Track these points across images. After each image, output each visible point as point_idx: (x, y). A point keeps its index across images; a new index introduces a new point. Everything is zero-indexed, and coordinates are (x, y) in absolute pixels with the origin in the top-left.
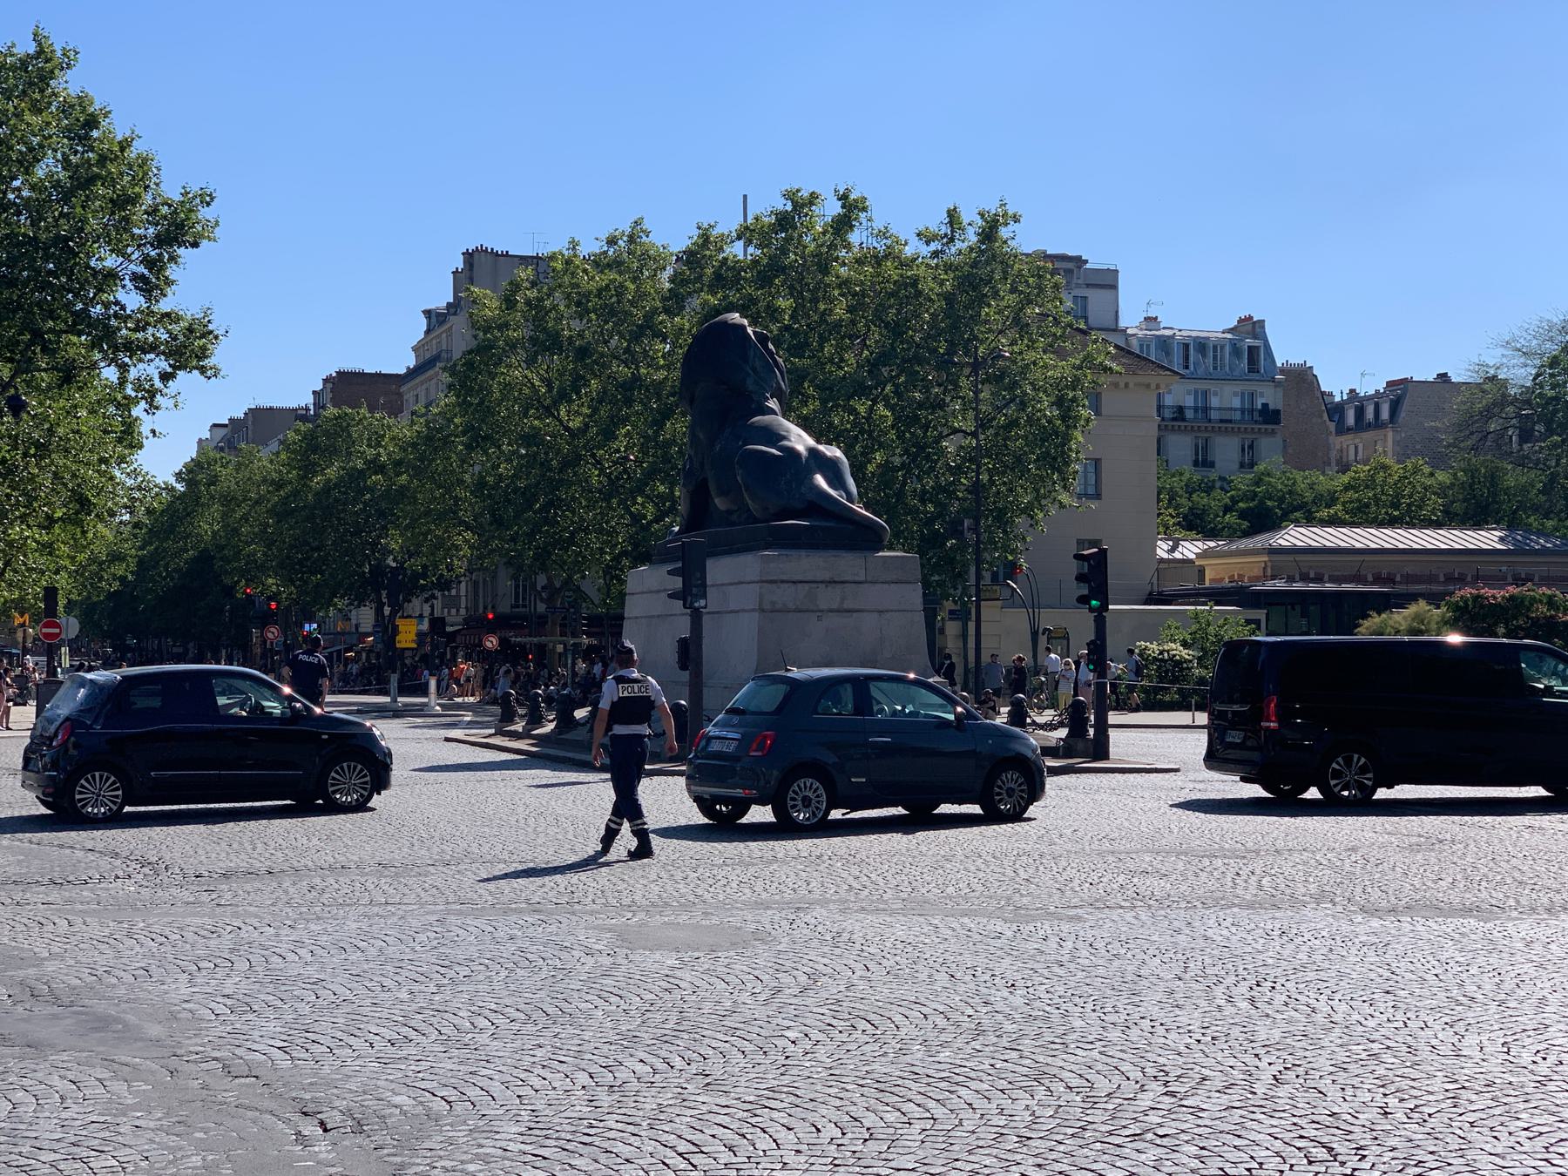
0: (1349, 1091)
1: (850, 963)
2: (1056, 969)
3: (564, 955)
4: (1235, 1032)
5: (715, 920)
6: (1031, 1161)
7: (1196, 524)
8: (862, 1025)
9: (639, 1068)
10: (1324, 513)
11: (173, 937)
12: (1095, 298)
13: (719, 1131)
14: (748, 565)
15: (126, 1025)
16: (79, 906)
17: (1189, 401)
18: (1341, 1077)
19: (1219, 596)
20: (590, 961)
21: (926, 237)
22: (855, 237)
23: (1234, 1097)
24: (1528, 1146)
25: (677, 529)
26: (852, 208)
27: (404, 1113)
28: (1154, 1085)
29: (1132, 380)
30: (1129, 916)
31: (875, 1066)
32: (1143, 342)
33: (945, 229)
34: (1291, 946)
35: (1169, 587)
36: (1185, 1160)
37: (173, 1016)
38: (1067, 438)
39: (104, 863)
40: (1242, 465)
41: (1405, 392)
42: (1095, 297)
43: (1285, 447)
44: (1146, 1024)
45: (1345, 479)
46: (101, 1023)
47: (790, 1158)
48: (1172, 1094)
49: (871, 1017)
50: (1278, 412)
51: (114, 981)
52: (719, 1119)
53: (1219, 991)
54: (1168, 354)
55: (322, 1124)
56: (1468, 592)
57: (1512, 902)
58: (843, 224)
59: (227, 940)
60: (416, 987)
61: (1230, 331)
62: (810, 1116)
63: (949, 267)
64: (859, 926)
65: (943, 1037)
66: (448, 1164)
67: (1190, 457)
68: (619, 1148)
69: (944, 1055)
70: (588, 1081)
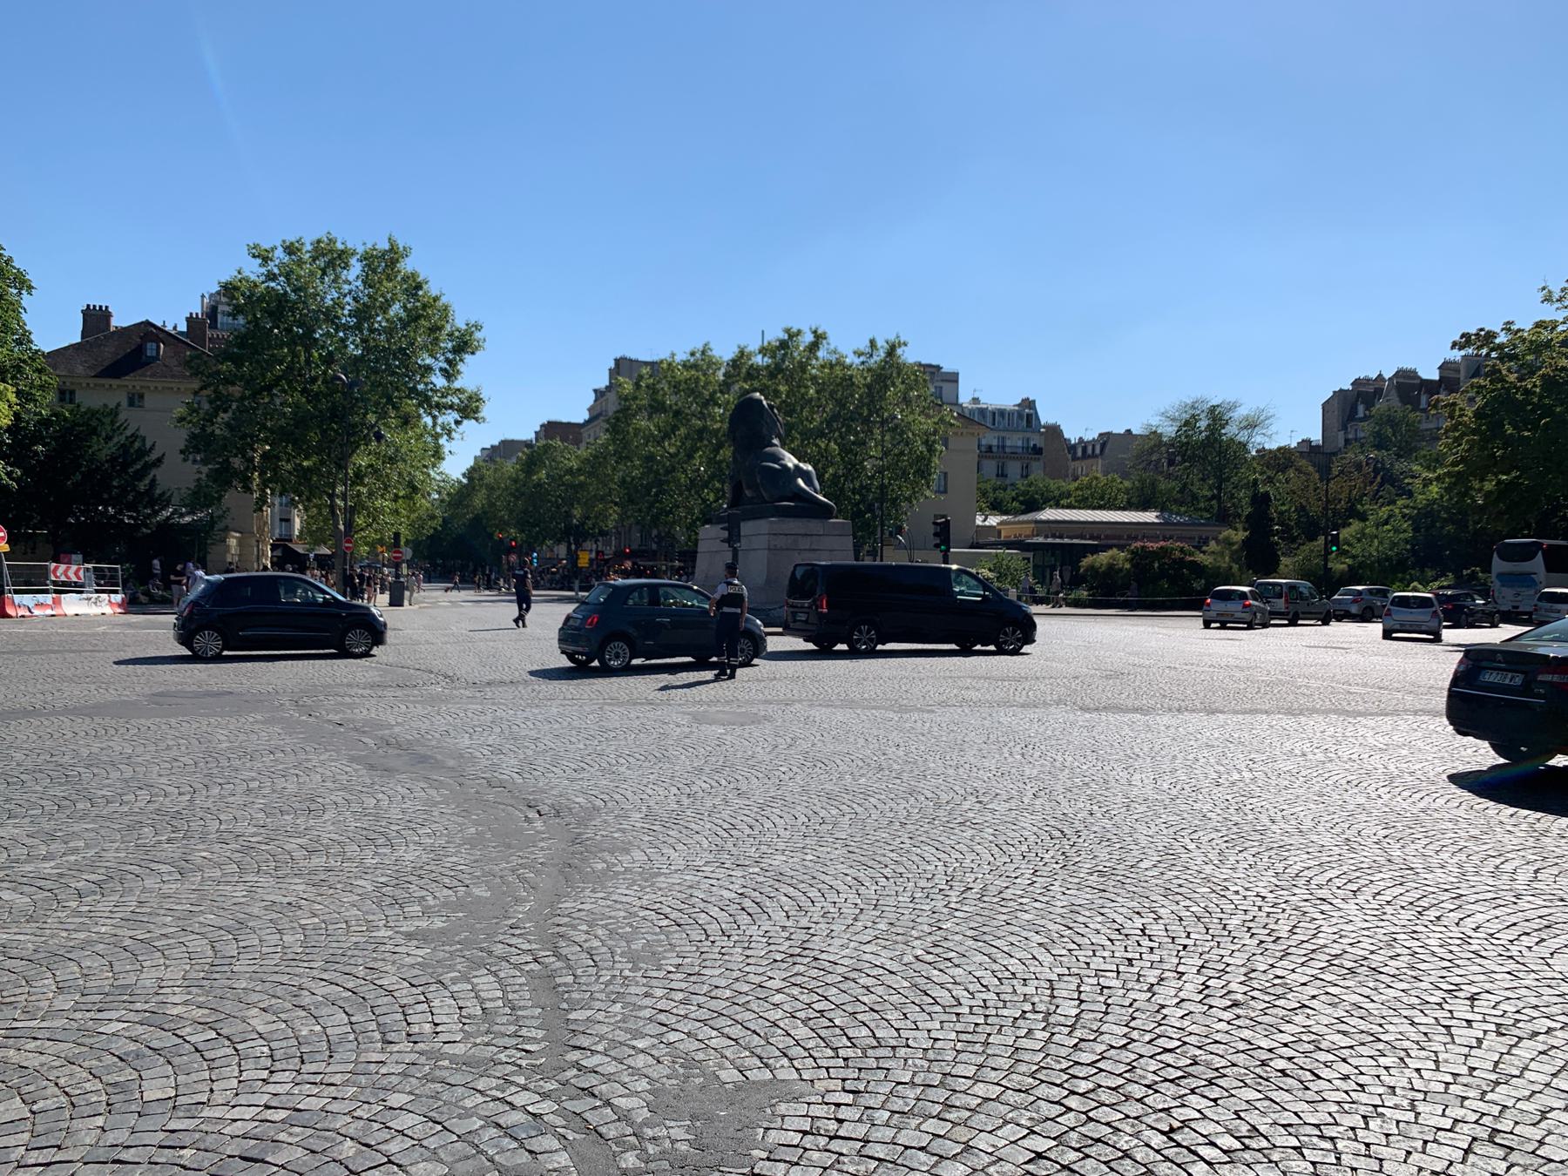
0: (1073, 802)
1: (814, 732)
2: (920, 737)
3: (664, 727)
4: (1013, 770)
5: (744, 710)
6: (906, 835)
7: (997, 507)
8: (819, 765)
9: (704, 785)
11: (461, 715)
13: (745, 818)
14: (763, 525)
15: (436, 760)
16: (411, 698)
17: (995, 443)
18: (1069, 795)
19: (1008, 545)
20: (679, 730)
21: (859, 354)
22: (820, 354)
23: (1013, 804)
24: (1165, 831)
25: (725, 506)
26: (819, 337)
27: (581, 807)
28: (971, 798)
29: (965, 431)
30: (959, 710)
31: (826, 786)
32: (971, 411)
33: (868, 350)
34: (1043, 727)
36: (987, 836)
37: (461, 756)
38: (930, 461)
39: (425, 676)
42: (946, 386)
43: (1045, 467)
44: (967, 766)
46: (423, 759)
47: (782, 832)
48: (980, 802)
49: (827, 762)
50: (1041, 449)
51: (430, 737)
52: (745, 812)
53: (1005, 750)
54: (984, 417)
55: (539, 812)
56: (1139, 544)
57: (1159, 706)
58: (814, 347)
59: (489, 717)
60: (588, 742)
61: (1019, 405)
62: (792, 811)
63: (869, 370)
64: (818, 713)
65: (861, 771)
66: (604, 833)
68: (693, 826)
69: (863, 780)
70: (676, 792)
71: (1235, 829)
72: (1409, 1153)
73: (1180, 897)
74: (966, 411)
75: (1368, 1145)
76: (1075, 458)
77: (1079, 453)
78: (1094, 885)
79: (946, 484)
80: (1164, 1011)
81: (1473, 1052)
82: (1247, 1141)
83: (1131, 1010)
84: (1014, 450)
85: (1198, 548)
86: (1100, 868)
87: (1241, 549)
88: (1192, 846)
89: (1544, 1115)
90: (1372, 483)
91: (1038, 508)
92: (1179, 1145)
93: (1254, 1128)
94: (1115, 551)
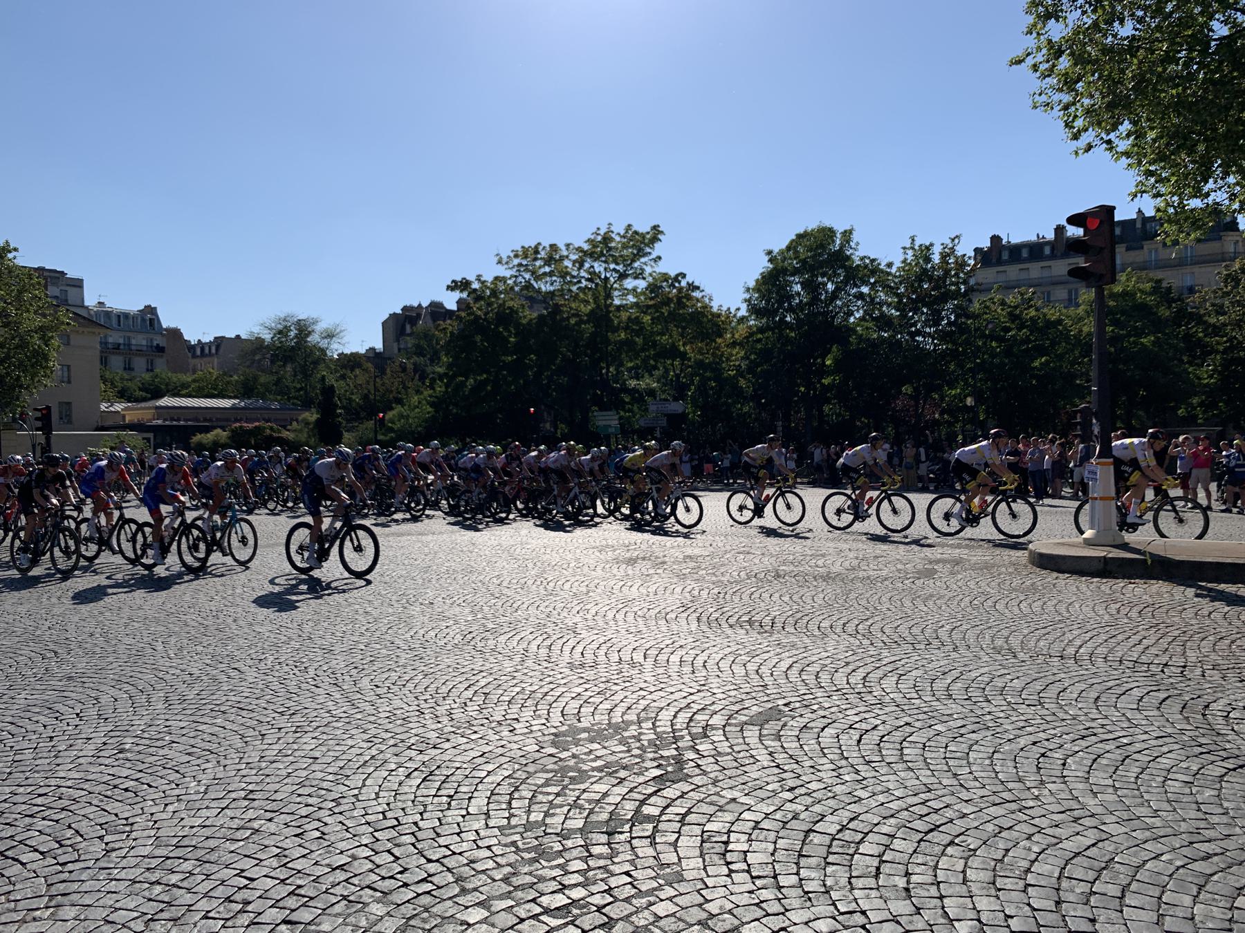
4: (43, 611)
7: (123, 395)
10: (183, 392)
12: (72, 292)
17: (121, 341)
29: (86, 330)
35: (107, 424)
40: (148, 370)
45: (194, 377)
56: (238, 425)
67: (123, 366)
71: (203, 630)
72: (182, 819)
73: (126, 685)
74: (92, 312)
75: (156, 822)
76: (194, 356)
77: (198, 352)
78: (58, 688)
79: (69, 377)
80: (58, 768)
82: (63, 842)
83: (28, 774)
84: (139, 348)
85: (284, 427)
86: (73, 675)
88: (160, 647)
89: (289, 775)
90: (413, 379)
91: (159, 395)
92: (7, 858)
93: (77, 832)
94: (219, 431)
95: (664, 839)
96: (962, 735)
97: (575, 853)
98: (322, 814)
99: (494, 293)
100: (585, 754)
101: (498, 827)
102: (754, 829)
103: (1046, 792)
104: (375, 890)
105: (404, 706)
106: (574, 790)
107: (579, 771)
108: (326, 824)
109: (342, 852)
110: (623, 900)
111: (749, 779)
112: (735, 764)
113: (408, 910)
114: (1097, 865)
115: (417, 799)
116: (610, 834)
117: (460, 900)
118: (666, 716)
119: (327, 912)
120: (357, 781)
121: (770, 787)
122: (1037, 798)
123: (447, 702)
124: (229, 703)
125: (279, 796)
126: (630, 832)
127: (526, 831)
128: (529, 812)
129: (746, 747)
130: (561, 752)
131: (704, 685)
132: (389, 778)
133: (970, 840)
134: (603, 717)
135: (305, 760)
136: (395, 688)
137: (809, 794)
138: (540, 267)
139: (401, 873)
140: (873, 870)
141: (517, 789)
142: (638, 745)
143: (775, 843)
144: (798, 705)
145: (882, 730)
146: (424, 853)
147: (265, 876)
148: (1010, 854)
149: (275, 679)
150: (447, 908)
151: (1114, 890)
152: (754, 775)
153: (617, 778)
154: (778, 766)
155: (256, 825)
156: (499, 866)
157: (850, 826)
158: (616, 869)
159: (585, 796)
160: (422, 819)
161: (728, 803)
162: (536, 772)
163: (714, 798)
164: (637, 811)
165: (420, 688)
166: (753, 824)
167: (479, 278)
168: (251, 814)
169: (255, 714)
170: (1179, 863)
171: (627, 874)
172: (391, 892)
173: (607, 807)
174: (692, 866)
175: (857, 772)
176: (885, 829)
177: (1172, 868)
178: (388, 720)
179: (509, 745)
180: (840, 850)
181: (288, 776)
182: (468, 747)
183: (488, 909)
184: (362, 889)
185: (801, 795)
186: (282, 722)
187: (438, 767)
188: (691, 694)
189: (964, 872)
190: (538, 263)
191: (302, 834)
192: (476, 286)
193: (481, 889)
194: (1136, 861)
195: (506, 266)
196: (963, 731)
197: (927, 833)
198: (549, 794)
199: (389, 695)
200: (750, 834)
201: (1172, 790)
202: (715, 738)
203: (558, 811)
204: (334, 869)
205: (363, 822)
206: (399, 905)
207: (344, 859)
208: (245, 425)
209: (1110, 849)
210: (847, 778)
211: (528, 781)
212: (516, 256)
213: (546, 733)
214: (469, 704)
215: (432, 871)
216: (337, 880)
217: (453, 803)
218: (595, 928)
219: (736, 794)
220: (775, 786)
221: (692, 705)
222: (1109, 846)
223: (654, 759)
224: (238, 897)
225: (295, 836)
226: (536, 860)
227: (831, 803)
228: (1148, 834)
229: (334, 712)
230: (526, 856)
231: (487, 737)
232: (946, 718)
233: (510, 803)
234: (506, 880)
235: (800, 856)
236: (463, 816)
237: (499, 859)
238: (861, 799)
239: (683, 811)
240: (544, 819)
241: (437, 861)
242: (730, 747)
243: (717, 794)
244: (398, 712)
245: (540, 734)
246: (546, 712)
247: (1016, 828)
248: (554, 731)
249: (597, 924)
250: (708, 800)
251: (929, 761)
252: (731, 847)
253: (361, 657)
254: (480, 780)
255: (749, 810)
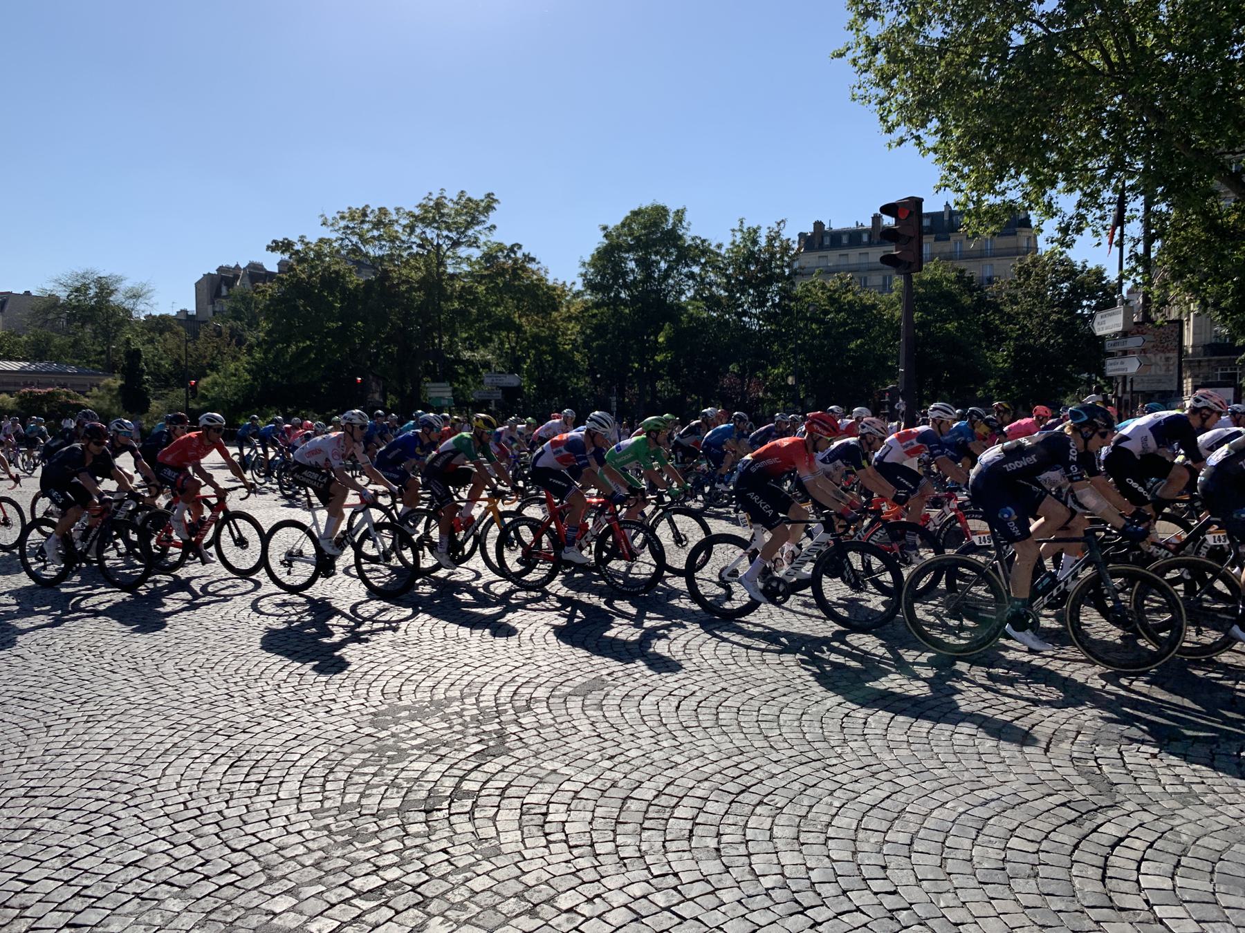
41: (8, 298)
56: (27, 390)
81: (58, 739)
85: (83, 393)
87: (117, 395)
90: (229, 345)
95: (483, 814)
96: (774, 699)
97: (391, 833)
98: (114, 808)
99: (319, 255)
100: (405, 732)
101: (310, 811)
102: (573, 799)
103: (848, 750)
104: (172, 885)
105: (212, 689)
106: (392, 769)
107: (399, 750)
108: (119, 819)
109: (136, 848)
110: (439, 878)
111: (570, 750)
112: (557, 735)
113: (209, 904)
114: (890, 816)
115: (223, 786)
116: (427, 812)
117: (266, 889)
118: (489, 691)
119: (117, 911)
120: (156, 770)
121: (590, 757)
122: (840, 756)
123: (260, 684)
124: (10, 694)
125: (64, 792)
126: (449, 808)
127: (340, 814)
128: (344, 794)
129: (569, 718)
130: (380, 731)
131: (529, 658)
132: (192, 766)
133: (777, 799)
134: (425, 695)
135: (97, 751)
136: (202, 672)
137: (627, 762)
138: (368, 231)
139: (202, 865)
140: (687, 833)
141: (331, 771)
142: (460, 721)
143: (593, 811)
144: (620, 674)
145: (700, 696)
146: (229, 843)
147: (46, 878)
148: (814, 810)
149: (65, 666)
150: (253, 899)
151: (904, 838)
152: (575, 746)
153: (437, 755)
154: (599, 736)
155: (37, 824)
156: (310, 851)
157: (666, 791)
158: (433, 847)
159: (403, 775)
160: (228, 808)
161: (548, 774)
162: (352, 753)
163: (535, 770)
164: (457, 787)
165: (230, 671)
166: (573, 794)
167: (302, 239)
168: (32, 812)
169: (40, 704)
170: (961, 810)
171: (445, 851)
172: (190, 886)
173: (426, 784)
174: (510, 839)
175: (675, 738)
176: (699, 793)
177: (955, 815)
178: (193, 705)
179: (324, 727)
180: (656, 816)
181: (76, 770)
182: (281, 729)
183: (296, 897)
184: (158, 885)
185: (620, 763)
186: (70, 711)
187: (248, 752)
188: (516, 668)
189: (771, 829)
190: (366, 226)
191: (90, 830)
192: (298, 247)
193: (289, 876)
194: (924, 810)
195: (331, 228)
196: (775, 694)
197: (738, 794)
198: (365, 774)
199: (196, 679)
200: (569, 805)
201: (958, 742)
202: (539, 711)
203: (374, 791)
204: (126, 866)
205: (162, 813)
206: (198, 899)
207: (138, 855)
208: (37, 390)
209: (903, 800)
210: (665, 744)
211: (344, 762)
212: (343, 218)
213: (365, 712)
214: (282, 685)
215: (236, 861)
216: (129, 878)
217: (262, 789)
218: (409, 908)
219: (556, 765)
220: (595, 755)
221: (517, 679)
222: (901, 798)
223: (476, 735)
224: (15, 902)
225: (82, 833)
226: (350, 843)
227: (650, 769)
228: (935, 785)
229: (132, 699)
230: (340, 839)
231: (301, 719)
232: (759, 683)
233: (324, 786)
234: (316, 865)
235: (617, 823)
236: (273, 802)
237: (310, 844)
238: (677, 764)
239: (503, 785)
240: (359, 801)
241: (243, 850)
242: (553, 719)
243: (538, 766)
244: (205, 696)
245: (358, 714)
246: (365, 691)
247: (820, 785)
248: (373, 710)
249: (411, 903)
250: (529, 772)
251: (742, 724)
252: (549, 818)
253: (165, 639)
254: (292, 763)
255: (569, 780)
